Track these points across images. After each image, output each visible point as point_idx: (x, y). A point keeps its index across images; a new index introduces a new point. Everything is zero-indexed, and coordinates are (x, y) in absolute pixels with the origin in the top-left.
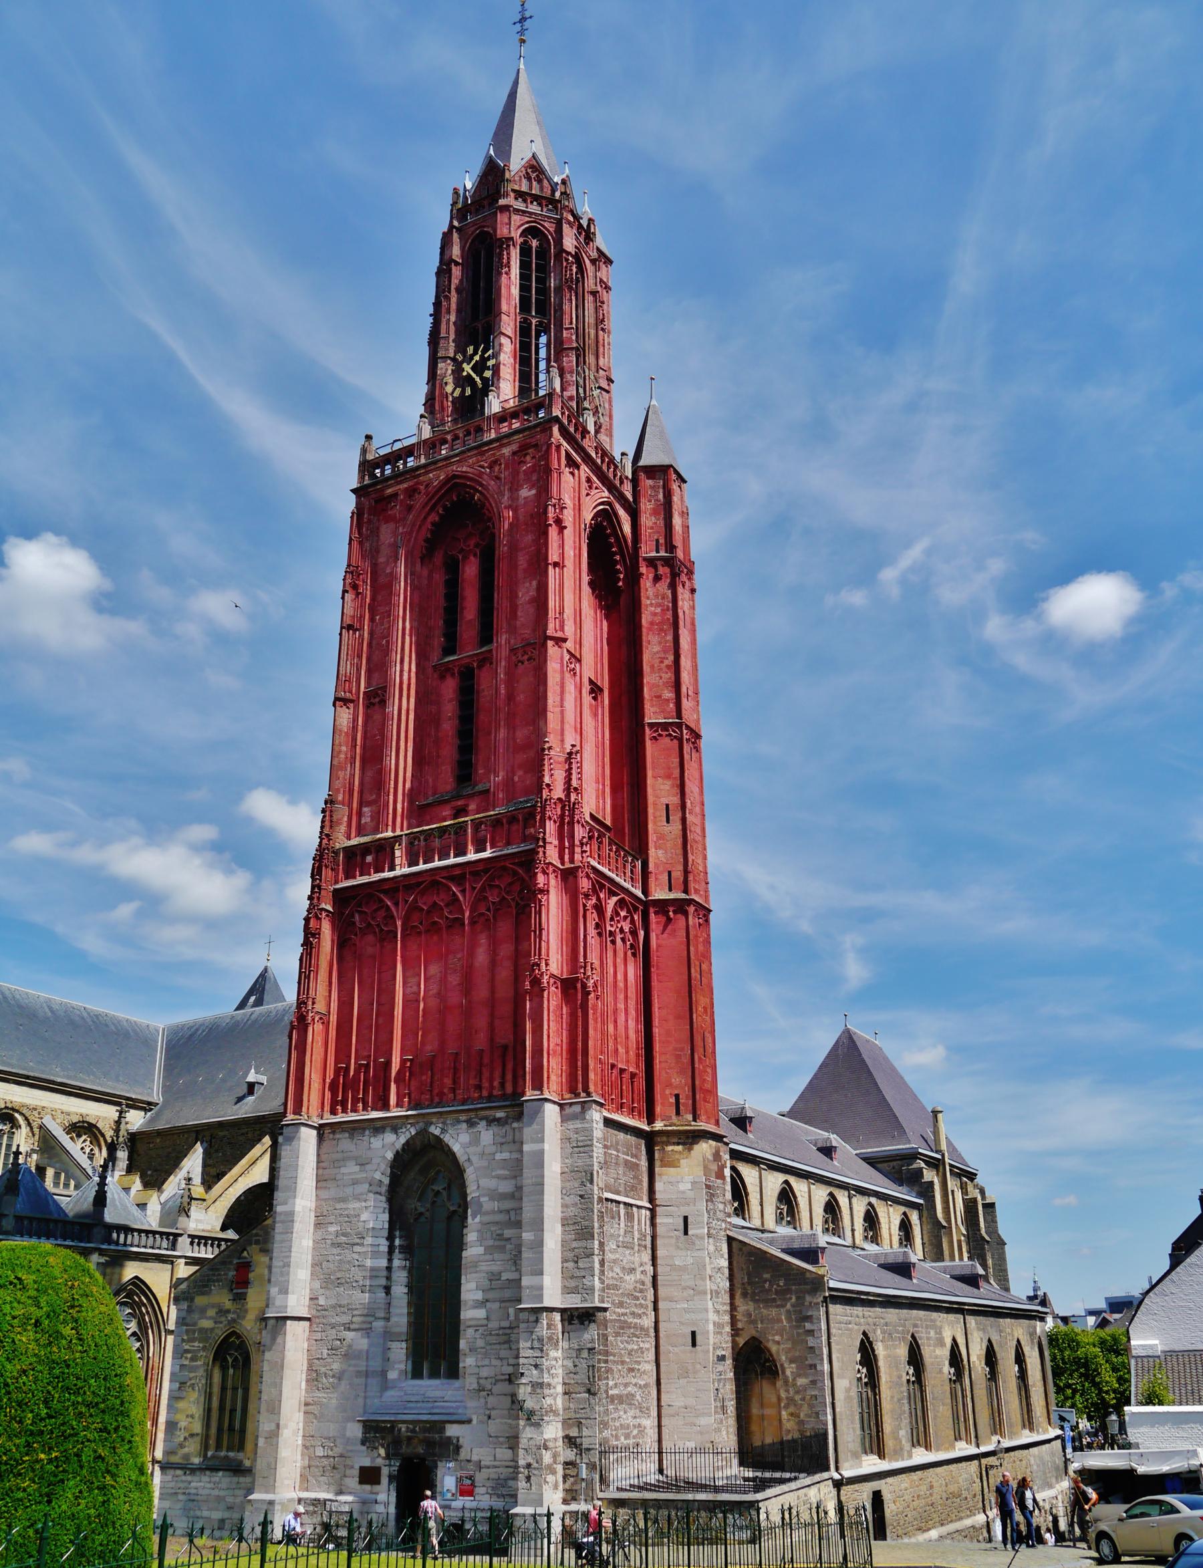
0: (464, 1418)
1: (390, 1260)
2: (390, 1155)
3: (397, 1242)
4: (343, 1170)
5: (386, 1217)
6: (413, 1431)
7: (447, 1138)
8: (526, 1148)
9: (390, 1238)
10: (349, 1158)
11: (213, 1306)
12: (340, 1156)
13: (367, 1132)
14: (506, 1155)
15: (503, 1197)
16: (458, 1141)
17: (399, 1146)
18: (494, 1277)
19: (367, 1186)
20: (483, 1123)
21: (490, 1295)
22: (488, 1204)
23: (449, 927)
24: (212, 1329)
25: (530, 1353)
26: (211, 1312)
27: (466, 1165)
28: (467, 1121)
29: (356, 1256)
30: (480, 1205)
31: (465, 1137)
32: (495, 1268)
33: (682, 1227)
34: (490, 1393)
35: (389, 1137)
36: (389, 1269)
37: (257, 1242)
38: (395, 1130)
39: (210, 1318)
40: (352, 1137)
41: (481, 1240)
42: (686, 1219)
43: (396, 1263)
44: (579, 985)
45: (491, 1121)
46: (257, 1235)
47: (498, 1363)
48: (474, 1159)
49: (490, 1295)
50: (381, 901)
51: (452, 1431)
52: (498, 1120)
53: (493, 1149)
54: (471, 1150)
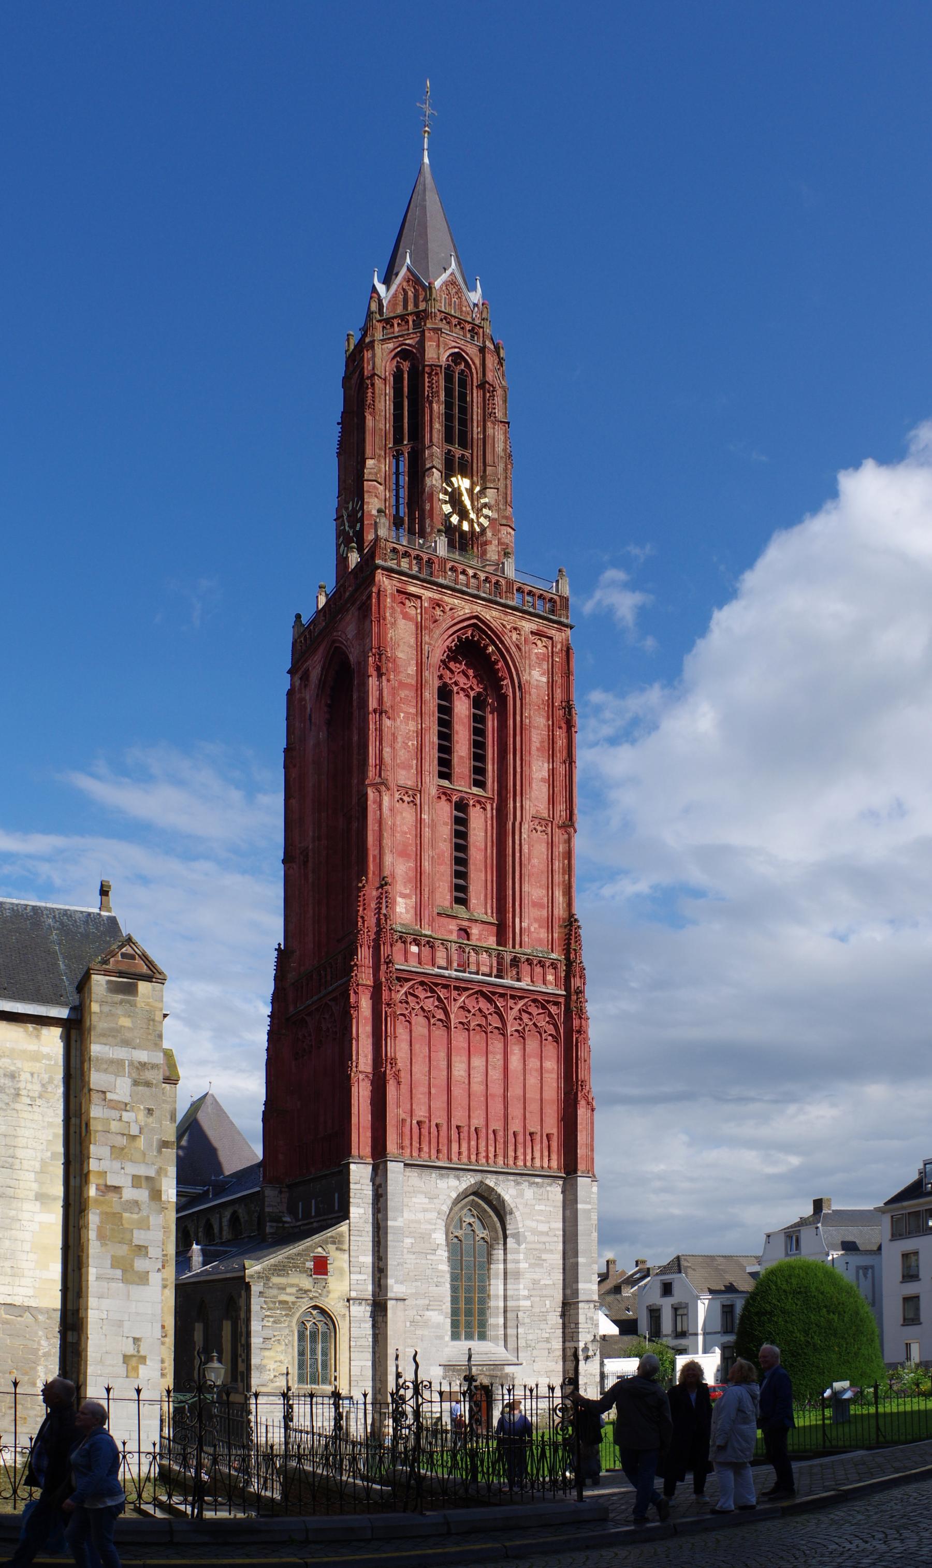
0: (517, 1362)
2: (454, 1195)
4: (414, 1200)
6: (482, 1370)
7: (499, 1190)
8: (580, 1206)
10: (419, 1192)
11: (292, 1286)
13: (434, 1175)
14: (542, 1207)
15: (542, 1233)
17: (461, 1190)
18: (535, 1282)
19: (436, 1214)
20: (527, 1184)
21: (534, 1293)
22: (530, 1237)
24: (294, 1303)
25: (586, 1326)
26: (294, 1290)
27: (514, 1210)
28: (514, 1181)
29: (430, 1262)
32: (536, 1277)
34: (534, 1348)
37: (334, 1243)
38: (458, 1178)
39: (290, 1294)
40: (420, 1176)
41: (526, 1259)
45: (532, 1184)
46: (332, 1237)
47: (539, 1332)
48: (520, 1207)
49: (534, 1293)
50: (435, 992)
51: (508, 1369)
52: (537, 1183)
53: (534, 1202)
54: (518, 1200)
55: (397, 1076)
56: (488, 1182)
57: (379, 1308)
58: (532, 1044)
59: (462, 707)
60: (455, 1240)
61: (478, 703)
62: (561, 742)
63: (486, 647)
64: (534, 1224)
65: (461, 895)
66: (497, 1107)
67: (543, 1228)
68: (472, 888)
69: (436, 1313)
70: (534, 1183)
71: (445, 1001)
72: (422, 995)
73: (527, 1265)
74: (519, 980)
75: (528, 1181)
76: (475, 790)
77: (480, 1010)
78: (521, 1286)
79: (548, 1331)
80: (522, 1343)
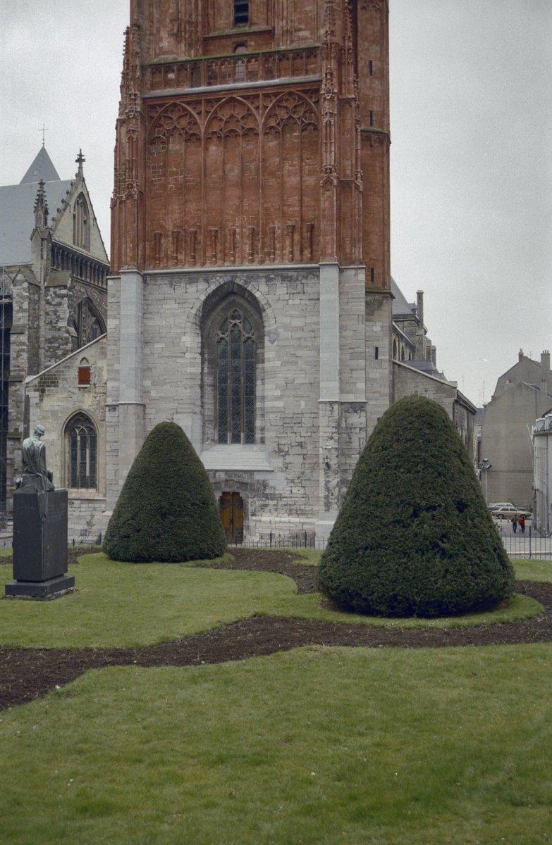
1: (202, 368)
2: (203, 297)
3: (206, 356)
5: (199, 339)
9: (202, 354)
12: (161, 297)
14: (297, 302)
16: (260, 291)
17: (210, 291)
19: (185, 318)
23: (244, 135)
27: (266, 307)
30: (278, 335)
31: (263, 288)
32: (290, 376)
33: (374, 355)
35: (202, 285)
36: (202, 373)
38: (207, 281)
42: (377, 349)
43: (206, 370)
44: (353, 185)
45: (284, 278)
50: (185, 109)
53: (287, 297)
56: (237, 281)
64: (287, 320)
67: (298, 322)
69: (185, 415)
70: (287, 277)
73: (278, 363)
75: (282, 276)
79: (303, 434)
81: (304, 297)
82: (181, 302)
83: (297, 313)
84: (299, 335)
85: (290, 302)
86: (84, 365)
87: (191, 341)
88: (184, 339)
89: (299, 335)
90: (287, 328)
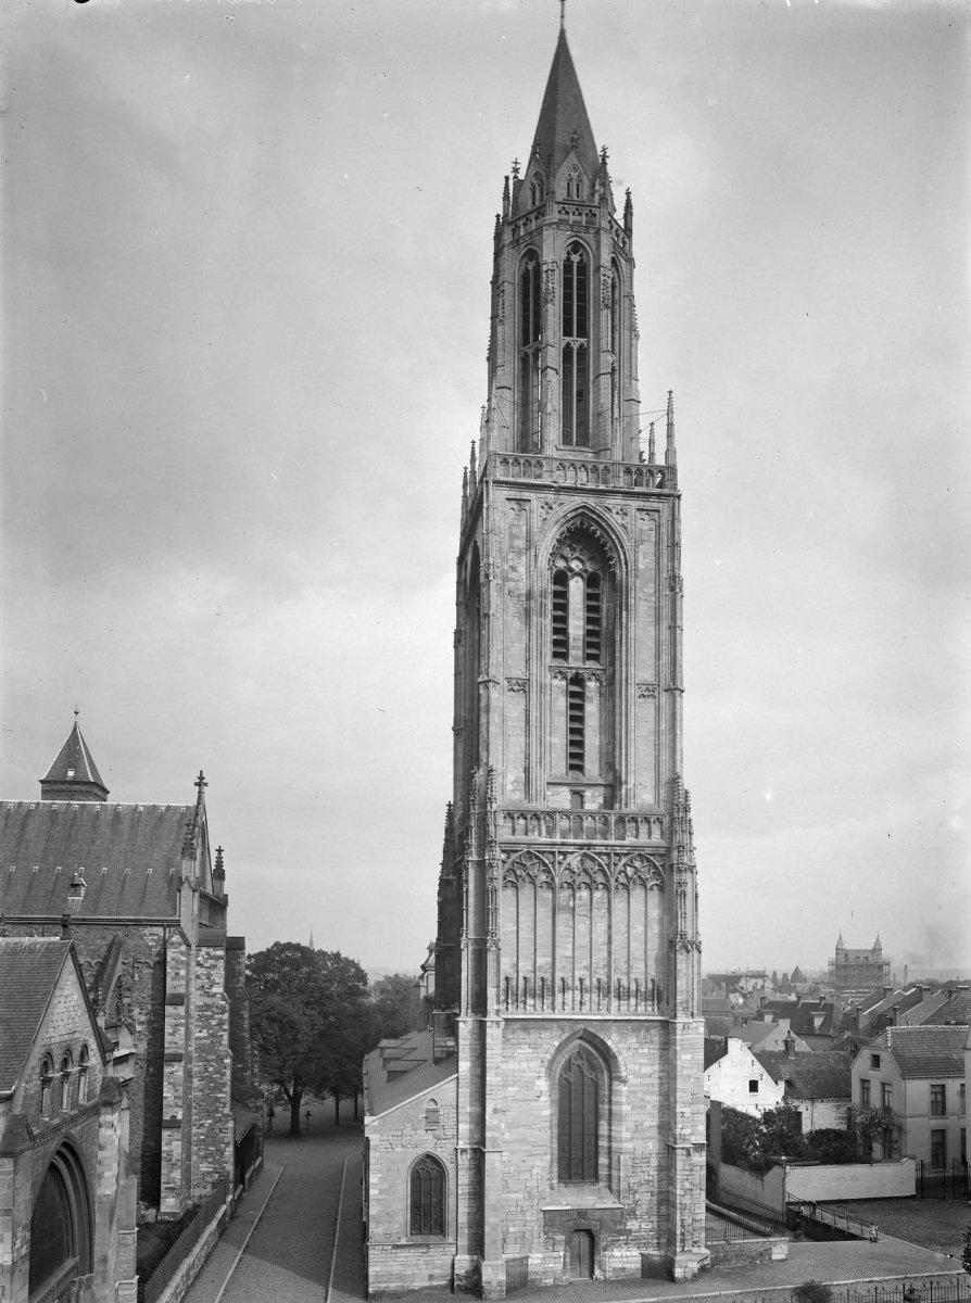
2: (557, 1044)
16: (612, 1041)
31: (615, 1037)
32: (639, 1118)
38: (562, 1029)
55: (496, 944)
57: (478, 1156)
58: (637, 893)
59: (576, 588)
60: (564, 1081)
61: (592, 581)
62: (666, 612)
63: (595, 532)
64: (637, 1068)
65: (576, 761)
66: (600, 956)
67: (646, 1070)
68: (587, 757)
71: (550, 866)
72: (528, 864)
74: (624, 839)
76: (591, 664)
77: (585, 870)
78: (624, 1129)
80: (623, 1185)
81: (652, 1046)
82: (535, 1047)
83: (647, 1062)
84: (648, 1081)
85: (640, 1051)
86: (433, 1106)
87: (543, 1084)
88: (538, 1082)
89: (648, 1081)
90: (637, 1075)
